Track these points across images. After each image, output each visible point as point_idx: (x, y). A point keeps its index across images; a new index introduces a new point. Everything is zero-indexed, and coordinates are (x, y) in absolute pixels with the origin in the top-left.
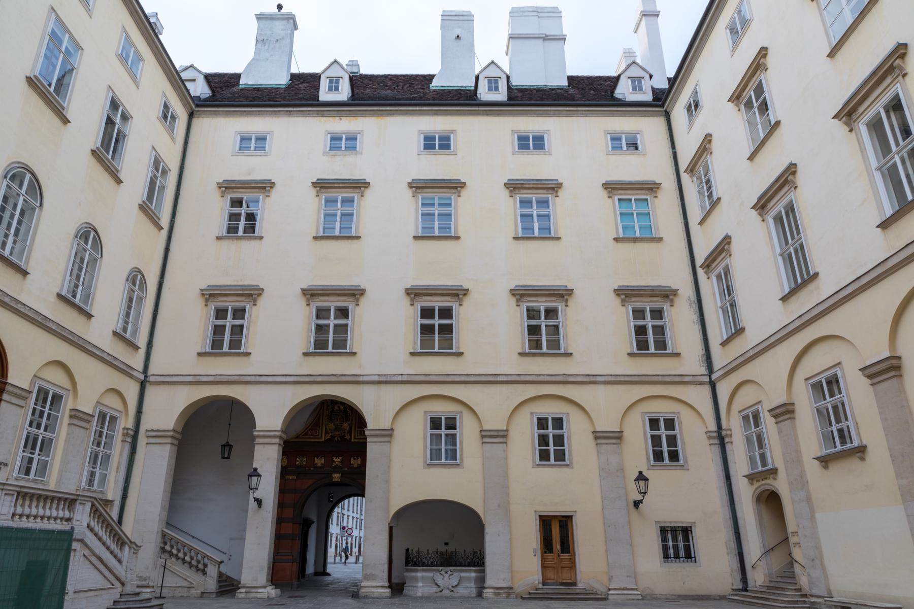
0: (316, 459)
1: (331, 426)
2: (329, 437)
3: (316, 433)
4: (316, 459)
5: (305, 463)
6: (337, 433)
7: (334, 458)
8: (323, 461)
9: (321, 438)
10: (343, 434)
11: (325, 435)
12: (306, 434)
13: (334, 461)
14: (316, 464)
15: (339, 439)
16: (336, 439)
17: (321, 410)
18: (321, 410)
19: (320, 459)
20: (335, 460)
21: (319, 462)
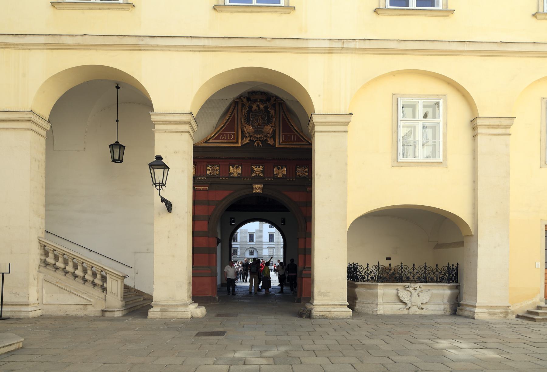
0: (231, 168)
1: (249, 129)
2: (247, 141)
3: (231, 137)
4: (231, 168)
5: (218, 173)
6: (258, 136)
7: (254, 167)
8: (239, 170)
9: (237, 143)
10: (265, 138)
11: (242, 139)
12: (217, 138)
13: (253, 171)
14: (232, 173)
15: (260, 143)
16: (256, 144)
17: (235, 111)
18: (235, 111)
19: (237, 167)
20: (255, 169)
21: (235, 171)
